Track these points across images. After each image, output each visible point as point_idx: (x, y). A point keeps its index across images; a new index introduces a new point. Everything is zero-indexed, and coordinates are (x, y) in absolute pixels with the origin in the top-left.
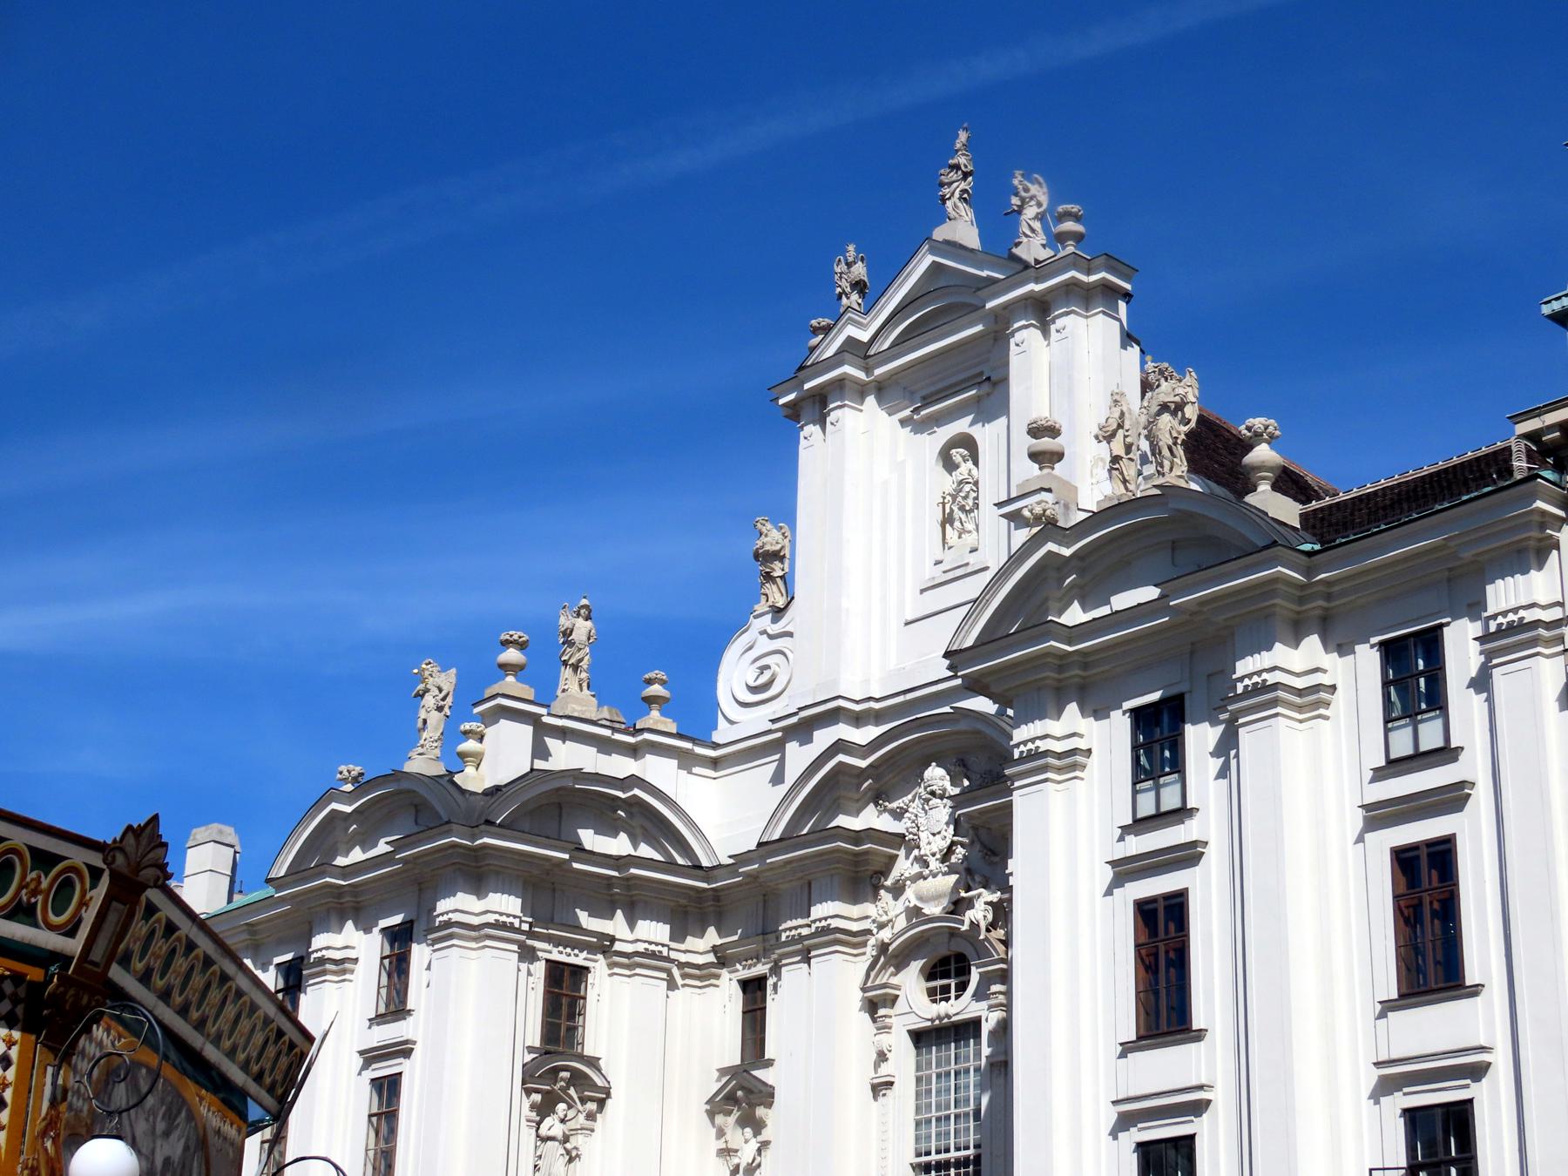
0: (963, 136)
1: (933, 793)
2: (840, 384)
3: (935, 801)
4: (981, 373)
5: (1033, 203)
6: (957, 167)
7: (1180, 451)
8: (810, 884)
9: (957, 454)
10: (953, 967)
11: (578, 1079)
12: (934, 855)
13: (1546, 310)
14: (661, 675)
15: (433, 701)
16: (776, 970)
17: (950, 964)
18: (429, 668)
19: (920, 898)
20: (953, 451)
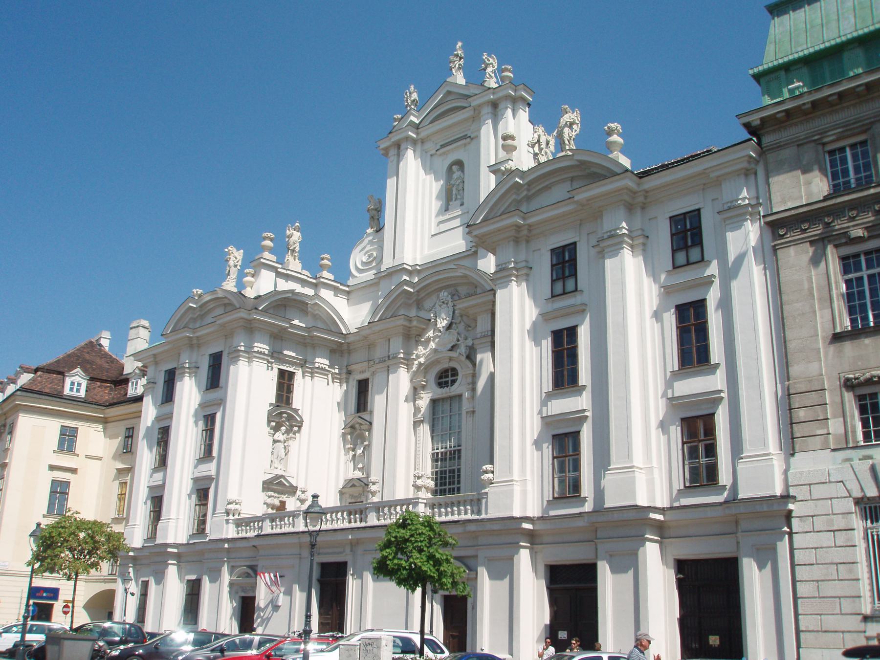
0: (460, 44)
4: (467, 135)
5: (491, 66)
6: (457, 55)
7: (572, 142)
8: (389, 340)
9: (455, 168)
10: (450, 374)
11: (290, 418)
13: (751, 72)
14: (328, 256)
15: (233, 262)
16: (373, 374)
18: (231, 248)
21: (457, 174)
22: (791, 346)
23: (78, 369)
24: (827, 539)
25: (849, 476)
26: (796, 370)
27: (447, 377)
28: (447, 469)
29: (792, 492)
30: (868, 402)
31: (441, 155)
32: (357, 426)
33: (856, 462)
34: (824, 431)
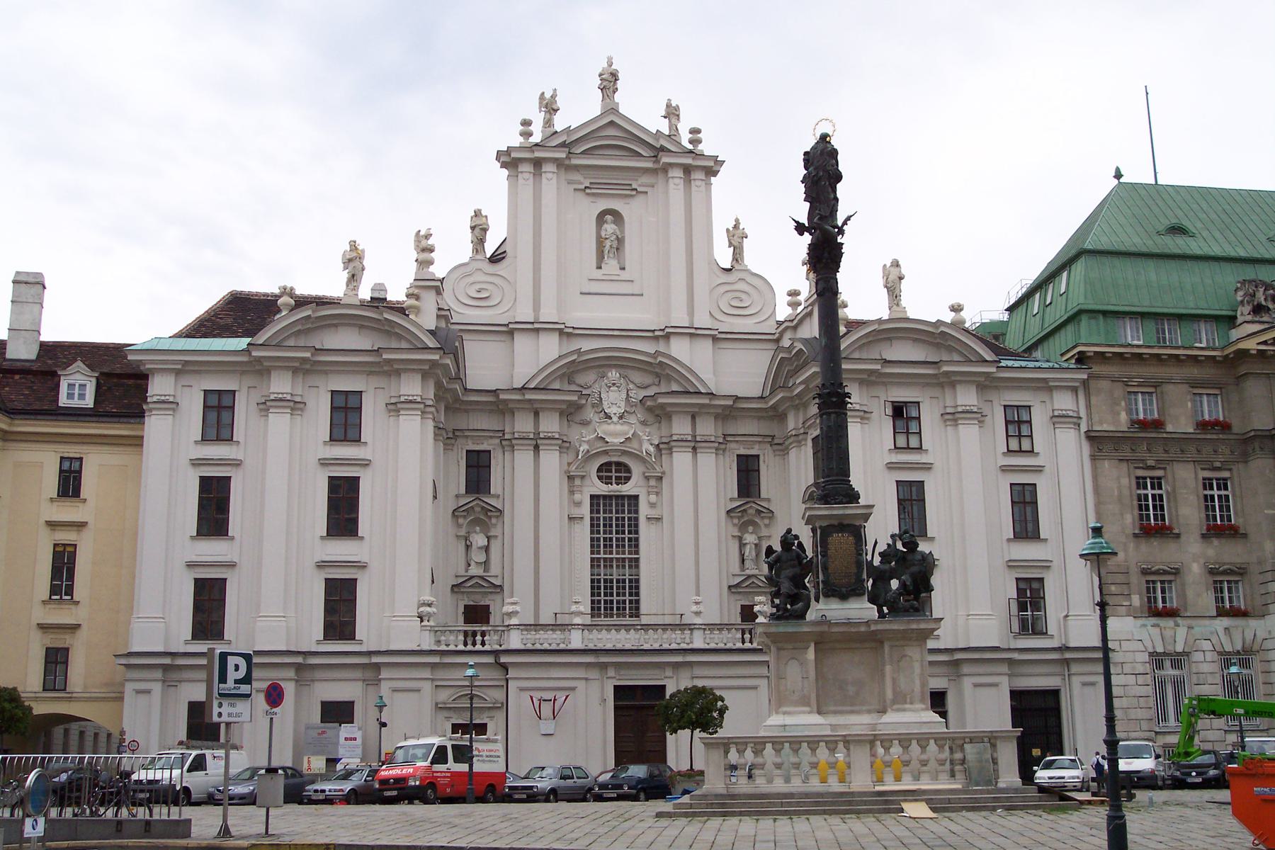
2: (555, 160)
4: (631, 185)
12: (615, 414)
17: (612, 466)
19: (605, 433)
21: (609, 228)
23: (79, 363)
24: (1131, 679)
25: (1145, 637)
28: (615, 577)
31: (588, 194)
32: (477, 509)
34: (1128, 603)
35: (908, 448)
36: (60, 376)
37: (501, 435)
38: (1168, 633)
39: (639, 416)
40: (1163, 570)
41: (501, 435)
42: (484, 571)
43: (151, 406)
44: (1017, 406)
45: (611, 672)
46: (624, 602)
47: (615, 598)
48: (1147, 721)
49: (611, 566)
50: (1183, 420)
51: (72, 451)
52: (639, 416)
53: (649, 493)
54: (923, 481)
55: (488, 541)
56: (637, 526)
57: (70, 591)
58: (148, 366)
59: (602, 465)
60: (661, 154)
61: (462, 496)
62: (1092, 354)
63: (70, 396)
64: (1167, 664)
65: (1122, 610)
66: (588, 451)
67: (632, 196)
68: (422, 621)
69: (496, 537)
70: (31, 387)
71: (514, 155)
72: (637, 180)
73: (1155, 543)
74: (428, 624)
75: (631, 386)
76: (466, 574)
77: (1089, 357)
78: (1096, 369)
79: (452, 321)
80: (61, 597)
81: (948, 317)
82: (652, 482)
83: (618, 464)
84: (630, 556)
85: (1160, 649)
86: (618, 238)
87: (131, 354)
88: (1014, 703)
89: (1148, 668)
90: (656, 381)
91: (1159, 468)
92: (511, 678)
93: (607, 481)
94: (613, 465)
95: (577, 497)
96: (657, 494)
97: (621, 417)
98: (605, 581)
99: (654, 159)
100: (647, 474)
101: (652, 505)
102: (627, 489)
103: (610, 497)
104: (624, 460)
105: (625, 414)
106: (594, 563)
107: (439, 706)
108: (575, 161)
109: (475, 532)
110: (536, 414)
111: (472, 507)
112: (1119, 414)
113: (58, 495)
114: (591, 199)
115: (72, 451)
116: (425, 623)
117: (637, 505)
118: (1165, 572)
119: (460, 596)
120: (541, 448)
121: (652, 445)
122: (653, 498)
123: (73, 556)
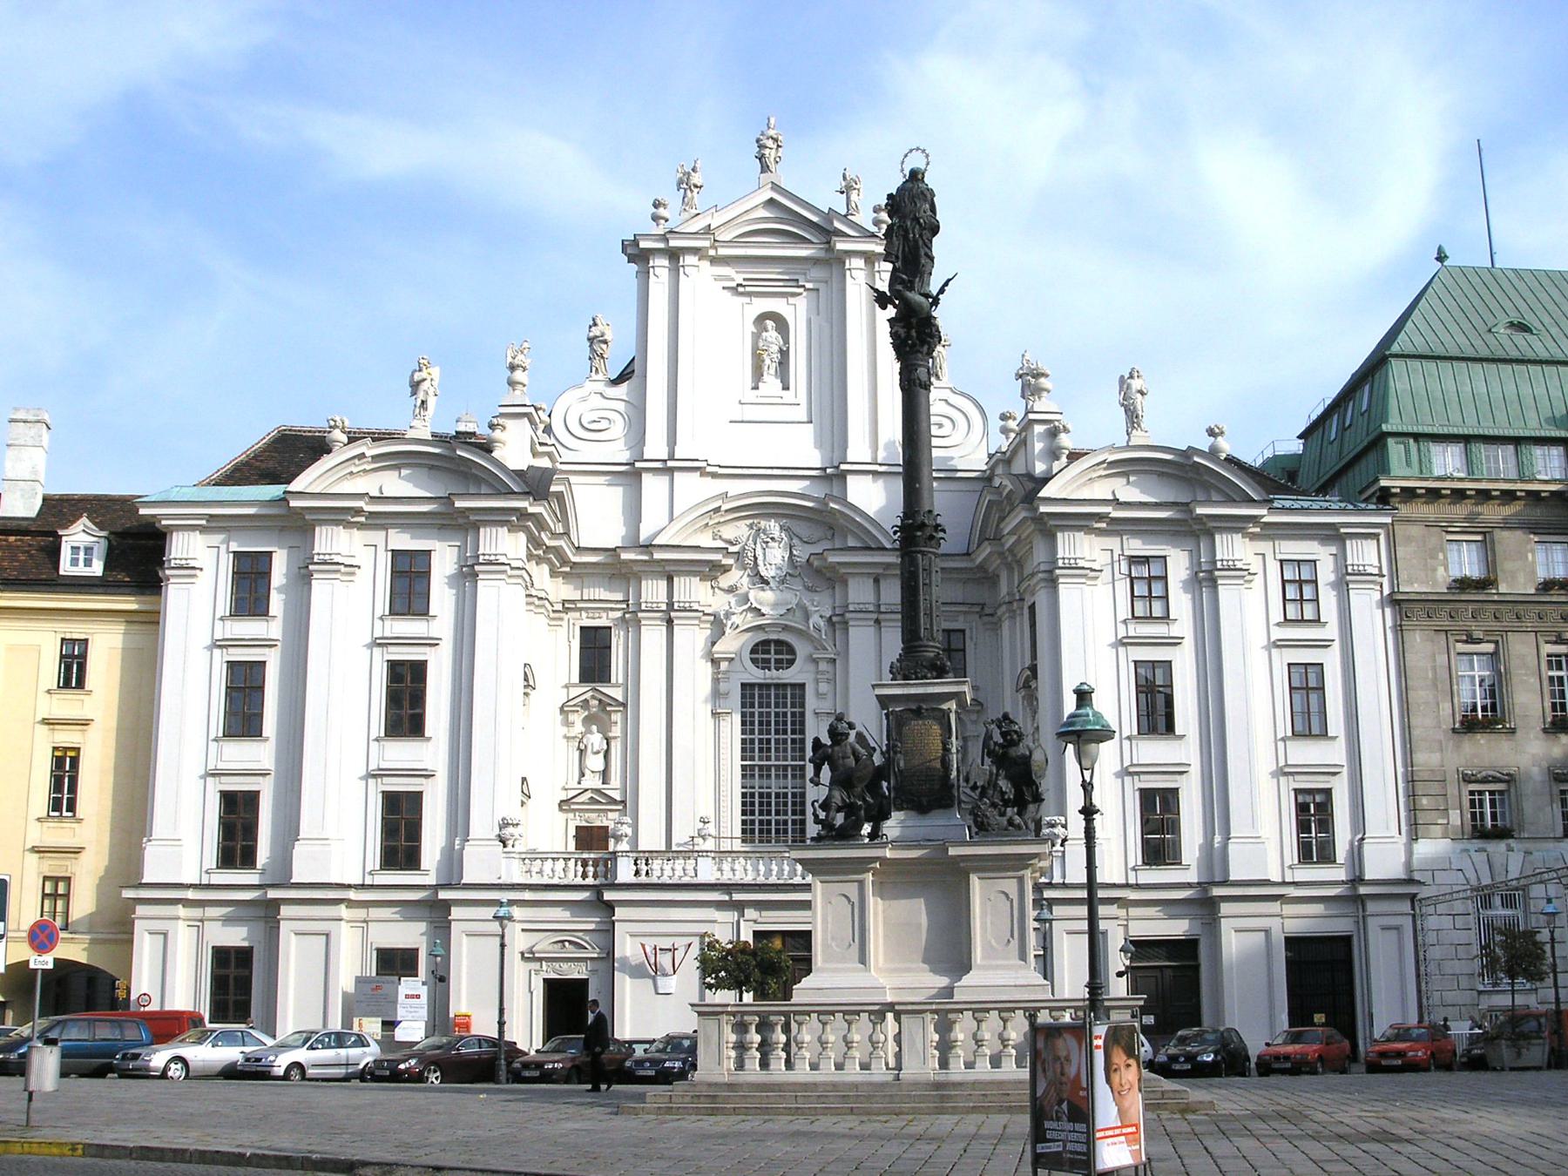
1: (773, 539)
2: (695, 251)
3: (771, 544)
4: (797, 280)
12: (772, 577)
19: (760, 604)
20: (768, 322)
21: (772, 335)
22: (1416, 733)
25: (1466, 865)
26: (1420, 758)
27: (768, 652)
28: (773, 791)
29: (1417, 876)
30: (1497, 797)
31: (742, 294)
33: (1473, 853)
34: (1445, 822)
35: (1151, 617)
36: (61, 536)
37: (625, 606)
38: (1498, 861)
39: (806, 580)
40: (1494, 777)
41: (625, 606)
42: (603, 783)
43: (168, 572)
44: (1299, 561)
45: (750, 913)
46: (785, 823)
47: (773, 818)
48: (1467, 977)
49: (769, 776)
50: (1521, 578)
51: (76, 630)
52: (806, 580)
53: (817, 681)
54: (1170, 662)
55: (608, 744)
56: (802, 723)
57: (72, 807)
58: (164, 522)
59: (757, 645)
60: (834, 238)
61: (574, 685)
62: (1398, 490)
63: (75, 562)
64: (1497, 901)
65: (1437, 830)
66: (737, 626)
67: (800, 294)
68: (505, 846)
69: (615, 738)
70: (28, 552)
71: (643, 245)
72: (805, 274)
73: (1482, 742)
74: (513, 850)
75: (795, 541)
76: (579, 786)
77: (1395, 495)
78: (1405, 510)
79: (560, 460)
80: (61, 815)
81: (1204, 443)
82: (823, 666)
83: (778, 643)
84: (777, 763)
85: (1486, 881)
86: (781, 351)
87: (143, 507)
88: (1289, 954)
89: (1470, 907)
90: (829, 534)
91: (1488, 642)
92: (618, 921)
93: (764, 665)
94: (773, 645)
95: (723, 687)
96: (828, 681)
97: (782, 582)
98: (761, 795)
99: (827, 246)
100: (814, 656)
101: (819, 695)
102: (788, 676)
103: (768, 686)
104: (784, 637)
105: (788, 578)
106: (747, 772)
107: (526, 955)
108: (723, 252)
109: (591, 732)
110: (670, 580)
111: (586, 701)
112: (1434, 570)
113: (59, 687)
114: (747, 300)
115: (76, 630)
116: (509, 849)
117: (803, 696)
118: (1496, 780)
119: (571, 815)
120: (676, 622)
121: (821, 617)
122: (823, 687)
123: (75, 762)
